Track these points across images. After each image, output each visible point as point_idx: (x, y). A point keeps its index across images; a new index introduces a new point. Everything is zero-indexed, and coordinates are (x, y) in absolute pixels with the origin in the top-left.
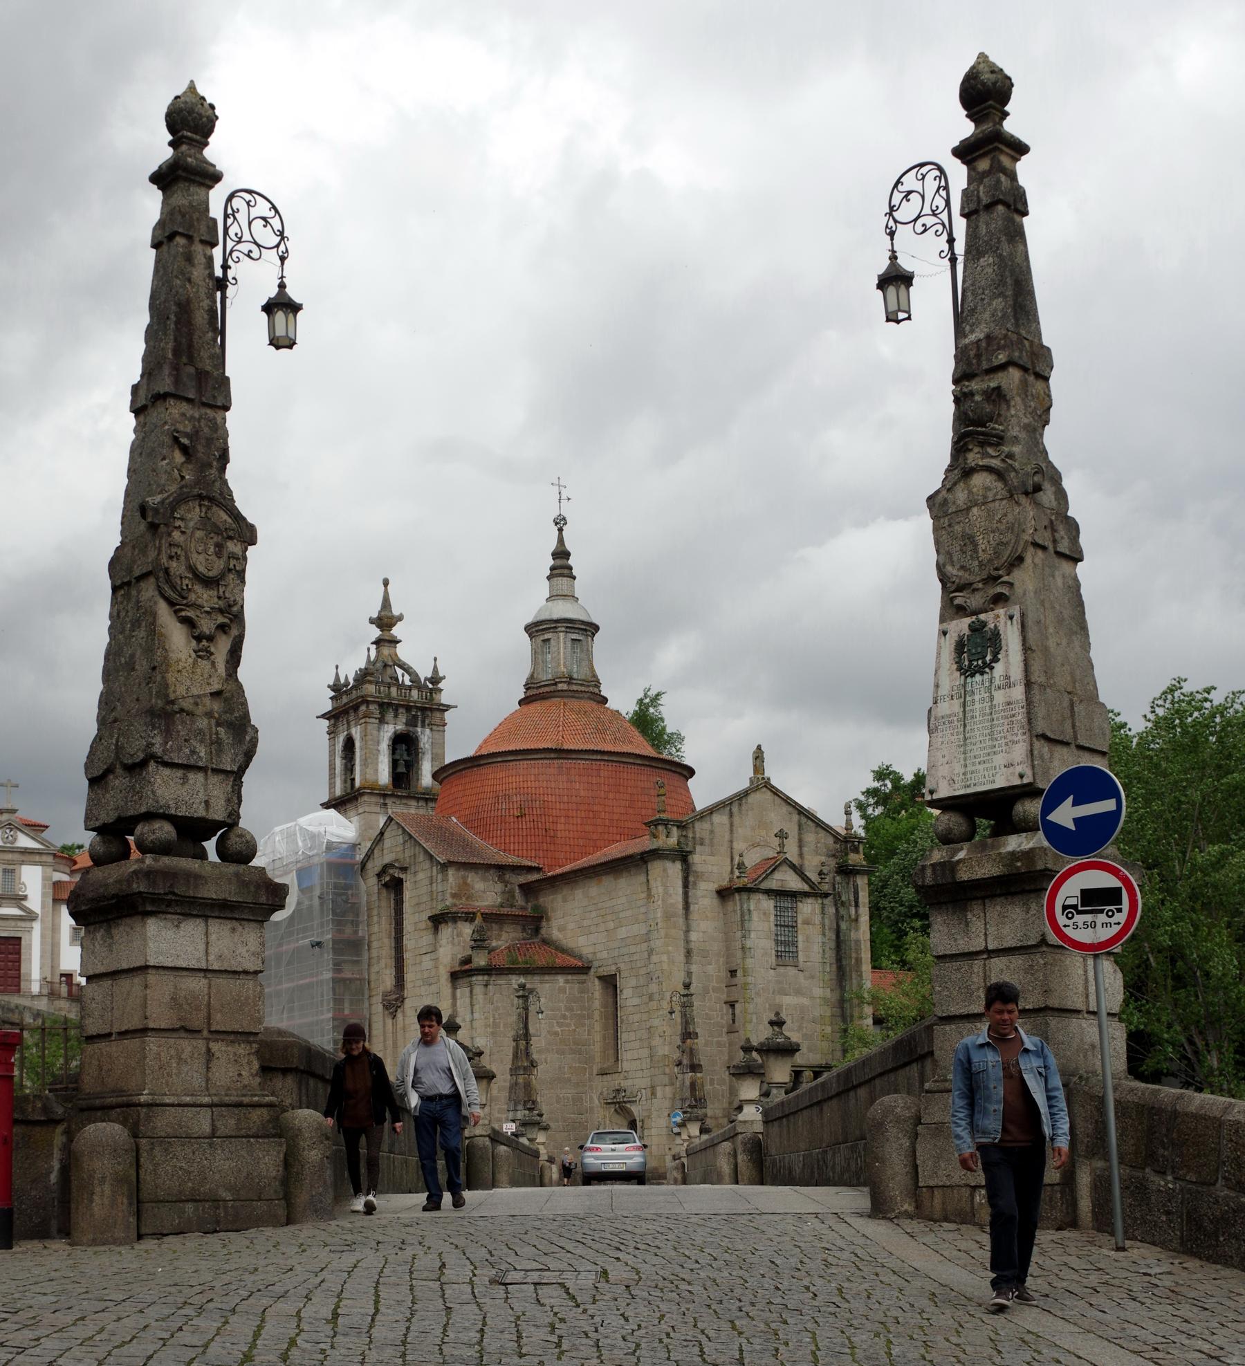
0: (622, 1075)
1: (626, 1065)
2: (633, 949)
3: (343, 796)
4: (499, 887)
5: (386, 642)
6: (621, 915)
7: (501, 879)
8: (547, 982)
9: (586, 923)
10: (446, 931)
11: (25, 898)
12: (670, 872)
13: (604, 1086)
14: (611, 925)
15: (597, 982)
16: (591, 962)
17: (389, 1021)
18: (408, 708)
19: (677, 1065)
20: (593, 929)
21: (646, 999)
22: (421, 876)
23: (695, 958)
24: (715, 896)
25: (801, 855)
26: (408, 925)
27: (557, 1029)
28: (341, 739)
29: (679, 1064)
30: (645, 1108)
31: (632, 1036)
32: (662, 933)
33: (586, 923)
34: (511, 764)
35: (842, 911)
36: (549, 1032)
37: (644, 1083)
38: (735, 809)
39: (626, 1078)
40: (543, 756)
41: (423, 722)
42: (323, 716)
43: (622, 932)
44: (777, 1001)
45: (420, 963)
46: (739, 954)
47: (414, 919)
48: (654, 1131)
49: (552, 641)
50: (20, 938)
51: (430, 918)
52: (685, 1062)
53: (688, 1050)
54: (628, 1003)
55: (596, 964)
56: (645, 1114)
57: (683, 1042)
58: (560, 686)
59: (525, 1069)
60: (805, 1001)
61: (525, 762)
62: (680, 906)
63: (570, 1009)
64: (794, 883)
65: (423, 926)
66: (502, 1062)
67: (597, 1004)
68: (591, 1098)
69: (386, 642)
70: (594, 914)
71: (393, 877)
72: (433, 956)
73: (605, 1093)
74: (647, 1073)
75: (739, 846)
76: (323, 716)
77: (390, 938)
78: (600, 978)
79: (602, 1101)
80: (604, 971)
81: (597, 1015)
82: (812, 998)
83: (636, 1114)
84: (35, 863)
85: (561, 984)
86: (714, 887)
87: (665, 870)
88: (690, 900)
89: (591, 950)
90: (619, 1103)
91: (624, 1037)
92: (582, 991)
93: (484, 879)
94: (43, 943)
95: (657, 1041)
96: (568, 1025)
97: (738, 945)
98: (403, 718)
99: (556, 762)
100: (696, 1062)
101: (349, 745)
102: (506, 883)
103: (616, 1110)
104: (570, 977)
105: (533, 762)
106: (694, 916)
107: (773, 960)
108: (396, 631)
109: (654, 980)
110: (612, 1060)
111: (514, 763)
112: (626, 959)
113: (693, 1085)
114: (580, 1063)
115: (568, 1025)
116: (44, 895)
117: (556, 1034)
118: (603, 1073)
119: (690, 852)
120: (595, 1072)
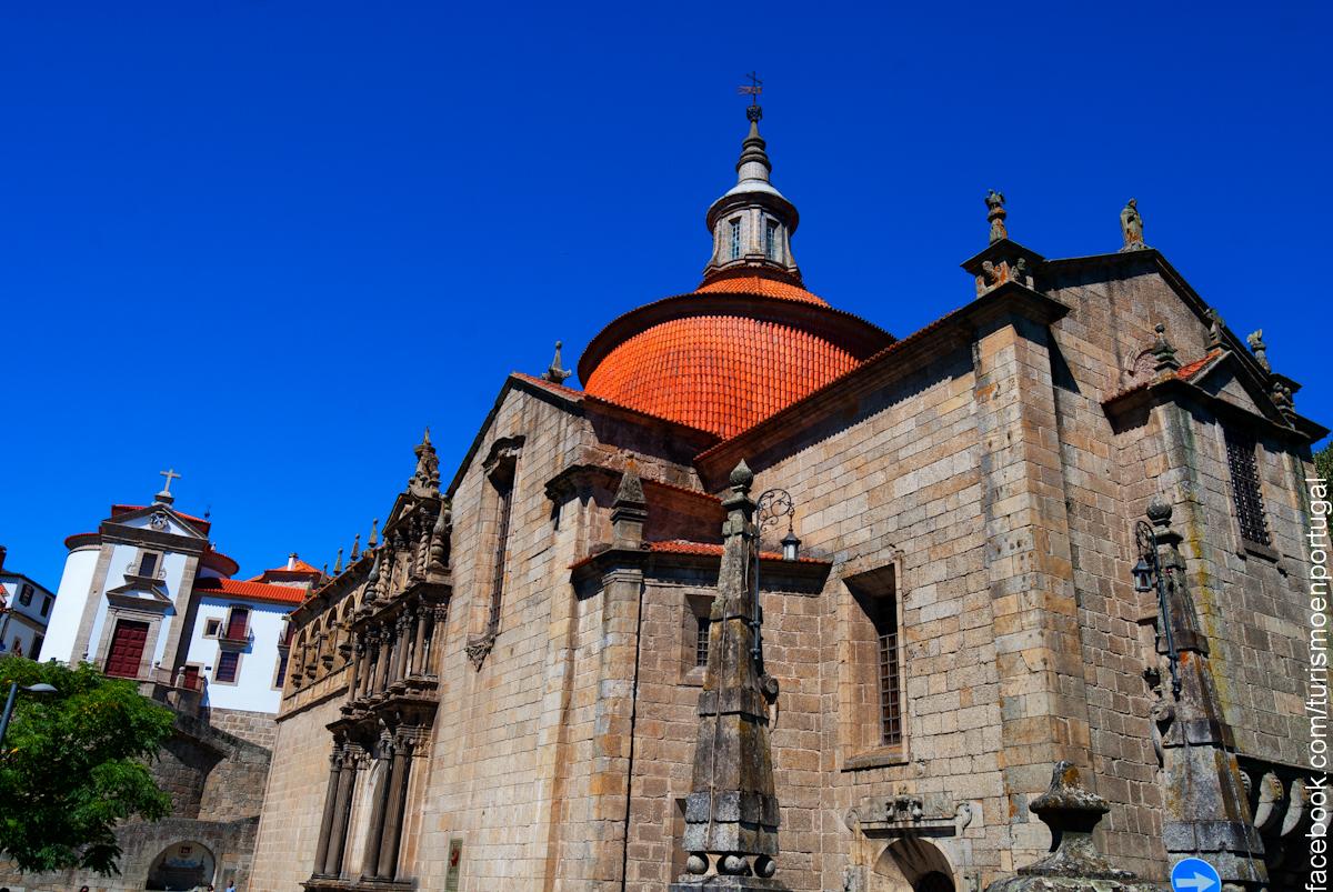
0: (909, 770)
1: (921, 748)
2: (935, 508)
6: (902, 454)
9: (817, 492)
10: (571, 508)
11: (162, 584)
13: (871, 795)
14: (880, 477)
17: (472, 674)
20: (834, 496)
21: (983, 598)
23: (1080, 520)
26: (516, 521)
30: (982, 844)
31: (939, 683)
33: (817, 492)
39: (921, 776)
43: (909, 483)
45: (526, 574)
49: (743, 220)
50: (146, 626)
52: (1188, 711)
54: (924, 616)
56: (981, 860)
58: (752, 264)
65: (536, 514)
66: (655, 732)
67: (844, 631)
68: (829, 821)
72: (546, 555)
73: (864, 809)
77: (490, 552)
79: (857, 827)
81: (843, 652)
86: (1099, 397)
91: (911, 686)
92: (812, 611)
94: (171, 632)
109: (1006, 550)
110: (875, 740)
114: (806, 746)
116: (184, 583)
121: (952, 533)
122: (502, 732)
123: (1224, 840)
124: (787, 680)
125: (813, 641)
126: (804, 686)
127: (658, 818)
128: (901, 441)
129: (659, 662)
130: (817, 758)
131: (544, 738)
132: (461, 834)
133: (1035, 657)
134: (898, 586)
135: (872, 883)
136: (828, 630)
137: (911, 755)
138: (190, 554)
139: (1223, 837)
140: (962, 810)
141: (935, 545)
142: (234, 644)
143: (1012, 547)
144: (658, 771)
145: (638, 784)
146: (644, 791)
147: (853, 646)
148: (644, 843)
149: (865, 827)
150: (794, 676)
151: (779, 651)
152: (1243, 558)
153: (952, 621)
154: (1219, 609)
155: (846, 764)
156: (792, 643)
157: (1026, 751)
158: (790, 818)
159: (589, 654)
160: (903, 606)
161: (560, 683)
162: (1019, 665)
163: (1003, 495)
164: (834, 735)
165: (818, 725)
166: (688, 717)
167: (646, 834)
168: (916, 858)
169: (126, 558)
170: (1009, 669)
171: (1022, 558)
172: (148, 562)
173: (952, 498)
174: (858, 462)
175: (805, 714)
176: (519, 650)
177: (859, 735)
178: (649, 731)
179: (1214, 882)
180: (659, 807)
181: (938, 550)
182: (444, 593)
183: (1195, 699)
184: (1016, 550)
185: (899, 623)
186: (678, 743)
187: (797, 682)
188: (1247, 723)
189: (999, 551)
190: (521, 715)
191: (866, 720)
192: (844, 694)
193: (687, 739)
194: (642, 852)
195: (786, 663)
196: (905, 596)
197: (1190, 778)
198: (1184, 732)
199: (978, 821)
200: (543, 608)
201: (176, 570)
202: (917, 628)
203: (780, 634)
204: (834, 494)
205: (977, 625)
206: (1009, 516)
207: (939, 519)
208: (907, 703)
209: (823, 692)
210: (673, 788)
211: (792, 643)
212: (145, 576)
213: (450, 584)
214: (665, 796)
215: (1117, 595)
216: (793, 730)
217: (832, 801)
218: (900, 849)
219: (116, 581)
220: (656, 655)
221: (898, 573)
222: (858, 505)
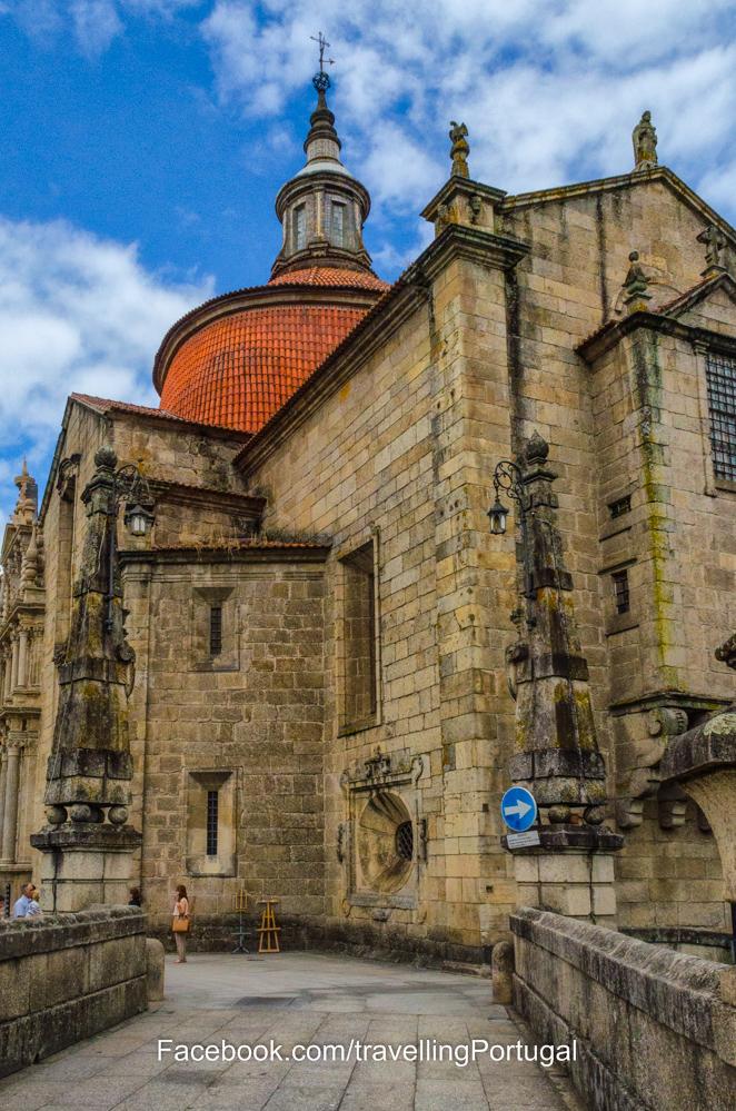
0: (382, 732)
1: (390, 711)
4: (200, 462)
6: (381, 428)
7: (204, 451)
8: (255, 576)
12: (481, 289)
13: (344, 758)
14: (365, 455)
15: (339, 569)
16: (331, 538)
19: (515, 661)
24: (573, 359)
27: (270, 658)
29: (520, 656)
30: (428, 793)
32: (464, 408)
34: (234, 316)
36: (254, 663)
37: (432, 739)
39: (390, 736)
40: (280, 299)
48: (449, 846)
53: (547, 617)
54: (396, 585)
55: (338, 539)
56: (429, 807)
57: (533, 596)
59: (93, 664)
61: (254, 311)
62: (503, 358)
63: (289, 624)
66: (169, 714)
70: (336, 454)
73: (352, 772)
74: (434, 719)
78: (346, 561)
80: (349, 547)
81: (338, 631)
83: (410, 808)
85: (278, 581)
87: (468, 282)
88: (522, 359)
89: (331, 517)
90: (377, 787)
93: (175, 448)
95: (455, 642)
96: (290, 652)
99: (298, 308)
100: (571, 650)
102: (213, 458)
103: (372, 804)
104: (294, 568)
105: (265, 310)
106: (532, 390)
109: (448, 514)
111: (239, 315)
113: (564, 710)
114: (309, 717)
115: (290, 652)
117: (268, 666)
118: (349, 732)
120: (336, 732)
121: (414, 506)
123: (553, 766)
124: (292, 660)
125: (319, 622)
126: (309, 665)
127: (174, 790)
128: (380, 415)
129: (171, 652)
130: (320, 729)
134: (376, 561)
135: (359, 835)
136: (329, 611)
137: (382, 718)
139: (553, 763)
140: (417, 762)
141: (402, 517)
143: (451, 508)
144: (173, 750)
145: (155, 762)
146: (161, 768)
147: (347, 623)
148: (161, 813)
149: (352, 786)
150: (299, 655)
151: (284, 634)
153: (412, 590)
154: (671, 551)
155: (340, 733)
156: (297, 626)
157: (455, 704)
158: (295, 783)
160: (379, 580)
162: (454, 623)
163: (446, 456)
164: (333, 706)
165: (321, 698)
166: (200, 700)
167: (162, 805)
168: (393, 811)
170: (446, 628)
171: (458, 519)
173: (415, 467)
174: (349, 443)
175: (309, 690)
177: (354, 704)
178: (164, 714)
179: (530, 807)
180: (175, 781)
181: (404, 520)
183: (545, 635)
184: (454, 511)
185: (376, 596)
186: (190, 724)
187: (302, 661)
188: (694, 662)
189: (442, 513)
191: (360, 691)
193: (199, 720)
194: (160, 821)
195: (291, 644)
196: (380, 569)
197: (534, 712)
198: (533, 669)
199: (426, 774)
202: (389, 599)
203: (285, 618)
204: (332, 480)
205: (430, 590)
206: (449, 478)
207: (405, 490)
208: (381, 671)
209: (326, 668)
210: (187, 763)
211: (297, 626)
213: (42, 601)
214: (180, 771)
215: (575, 548)
216: (298, 705)
217: (331, 766)
218: (378, 803)
220: (168, 646)
221: (375, 549)
222: (349, 487)
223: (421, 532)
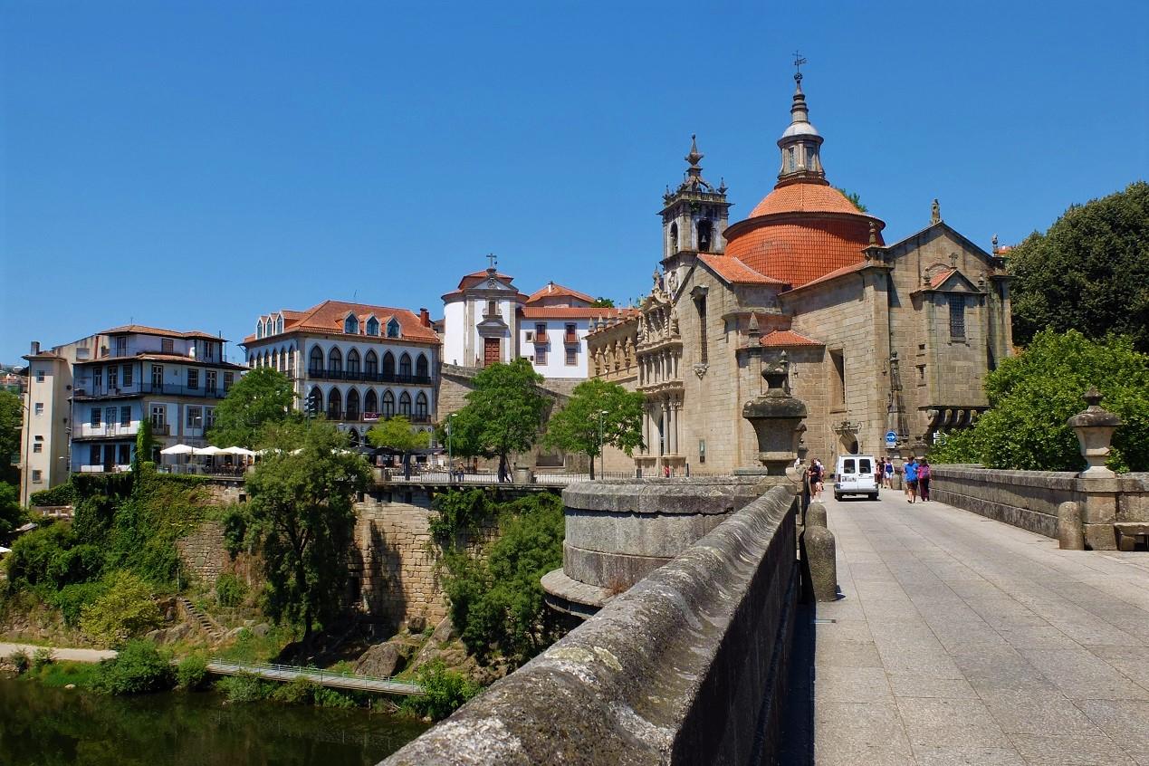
2: (853, 333)
3: (671, 257)
5: (694, 172)
6: (845, 311)
11: (501, 317)
13: (836, 421)
14: (839, 318)
18: (707, 207)
21: (864, 364)
22: (716, 292)
25: (965, 269)
28: (670, 225)
31: (854, 388)
35: (992, 305)
37: (865, 417)
38: (921, 241)
39: (850, 415)
41: (716, 213)
42: (660, 214)
43: (847, 322)
44: (952, 364)
46: (926, 334)
47: (713, 317)
51: (723, 318)
58: (800, 177)
60: (972, 364)
64: (960, 288)
69: (694, 172)
71: (700, 295)
75: (925, 265)
76: (660, 214)
80: (834, 347)
81: (829, 375)
82: (975, 362)
84: (507, 299)
89: (825, 334)
96: (811, 381)
97: (925, 328)
98: (704, 211)
101: (674, 229)
107: (948, 338)
108: (700, 164)
112: (850, 339)
119: (892, 269)
122: (716, 403)
131: (732, 406)
132: (704, 437)
133: (875, 384)
138: (511, 300)
142: (542, 348)
152: (950, 344)
159: (744, 380)
161: (736, 389)
169: (481, 306)
172: (492, 306)
176: (718, 374)
182: (679, 347)
190: (722, 397)
192: (830, 389)
200: (726, 360)
201: (505, 309)
212: (492, 315)
219: (479, 319)
223: (861, 353)
